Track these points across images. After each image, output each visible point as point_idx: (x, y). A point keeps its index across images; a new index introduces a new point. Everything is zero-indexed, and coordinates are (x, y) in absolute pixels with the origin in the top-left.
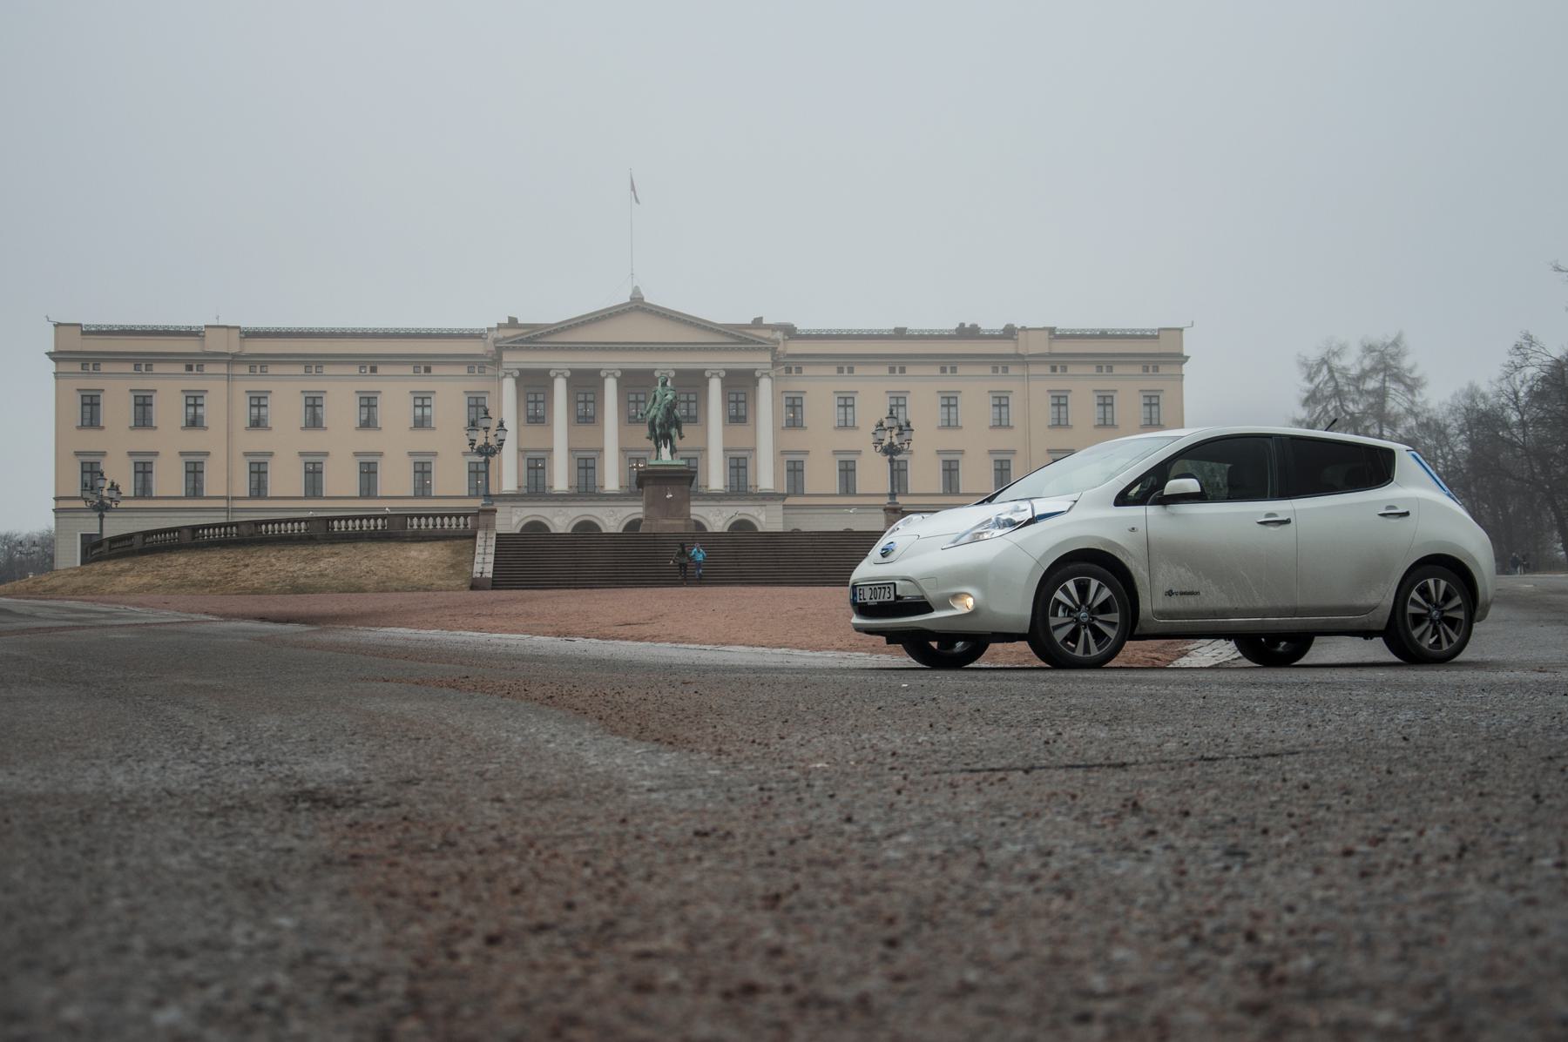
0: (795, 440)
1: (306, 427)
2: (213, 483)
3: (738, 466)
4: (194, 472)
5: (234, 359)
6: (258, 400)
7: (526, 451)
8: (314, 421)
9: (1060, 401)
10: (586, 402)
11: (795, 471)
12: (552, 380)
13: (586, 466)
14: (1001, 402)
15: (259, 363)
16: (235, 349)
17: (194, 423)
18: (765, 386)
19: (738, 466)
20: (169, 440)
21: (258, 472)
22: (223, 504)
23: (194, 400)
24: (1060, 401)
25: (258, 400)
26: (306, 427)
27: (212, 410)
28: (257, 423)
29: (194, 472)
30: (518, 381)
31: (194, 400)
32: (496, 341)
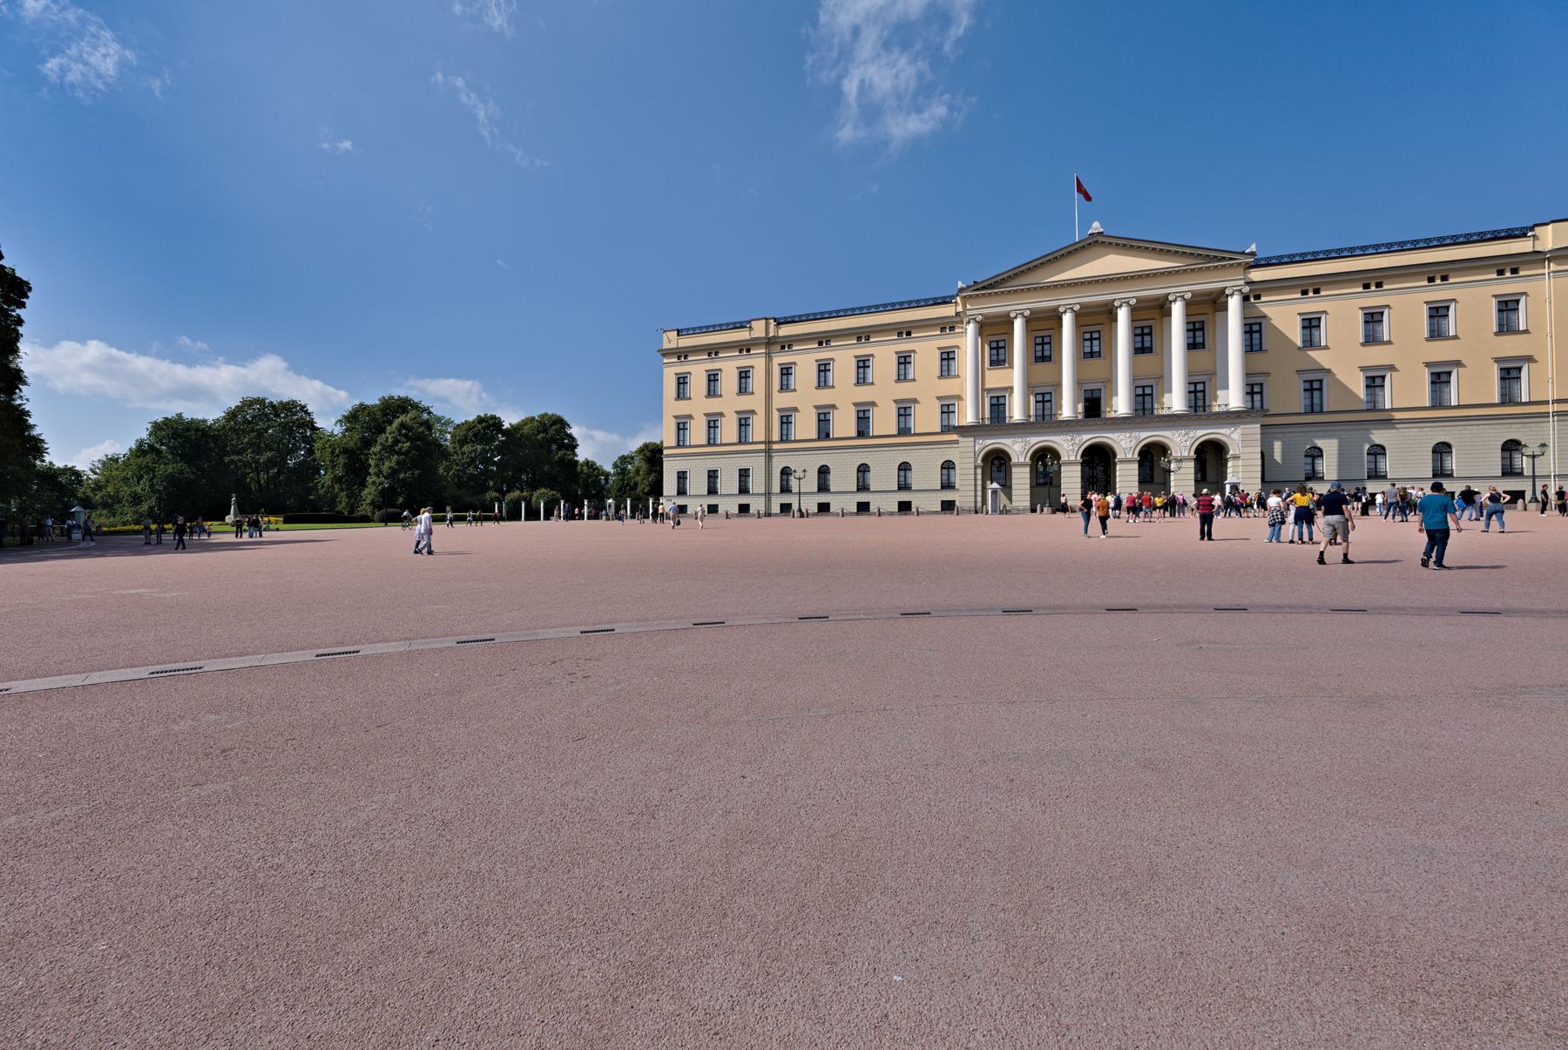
1: (819, 387)
2: (757, 431)
4: (743, 424)
5: (769, 342)
6: (786, 371)
7: (989, 390)
10: (1043, 344)
17: (743, 390)
20: (729, 402)
21: (786, 421)
22: (762, 447)
23: (744, 375)
26: (819, 387)
27: (757, 381)
28: (784, 387)
29: (743, 424)
31: (744, 375)
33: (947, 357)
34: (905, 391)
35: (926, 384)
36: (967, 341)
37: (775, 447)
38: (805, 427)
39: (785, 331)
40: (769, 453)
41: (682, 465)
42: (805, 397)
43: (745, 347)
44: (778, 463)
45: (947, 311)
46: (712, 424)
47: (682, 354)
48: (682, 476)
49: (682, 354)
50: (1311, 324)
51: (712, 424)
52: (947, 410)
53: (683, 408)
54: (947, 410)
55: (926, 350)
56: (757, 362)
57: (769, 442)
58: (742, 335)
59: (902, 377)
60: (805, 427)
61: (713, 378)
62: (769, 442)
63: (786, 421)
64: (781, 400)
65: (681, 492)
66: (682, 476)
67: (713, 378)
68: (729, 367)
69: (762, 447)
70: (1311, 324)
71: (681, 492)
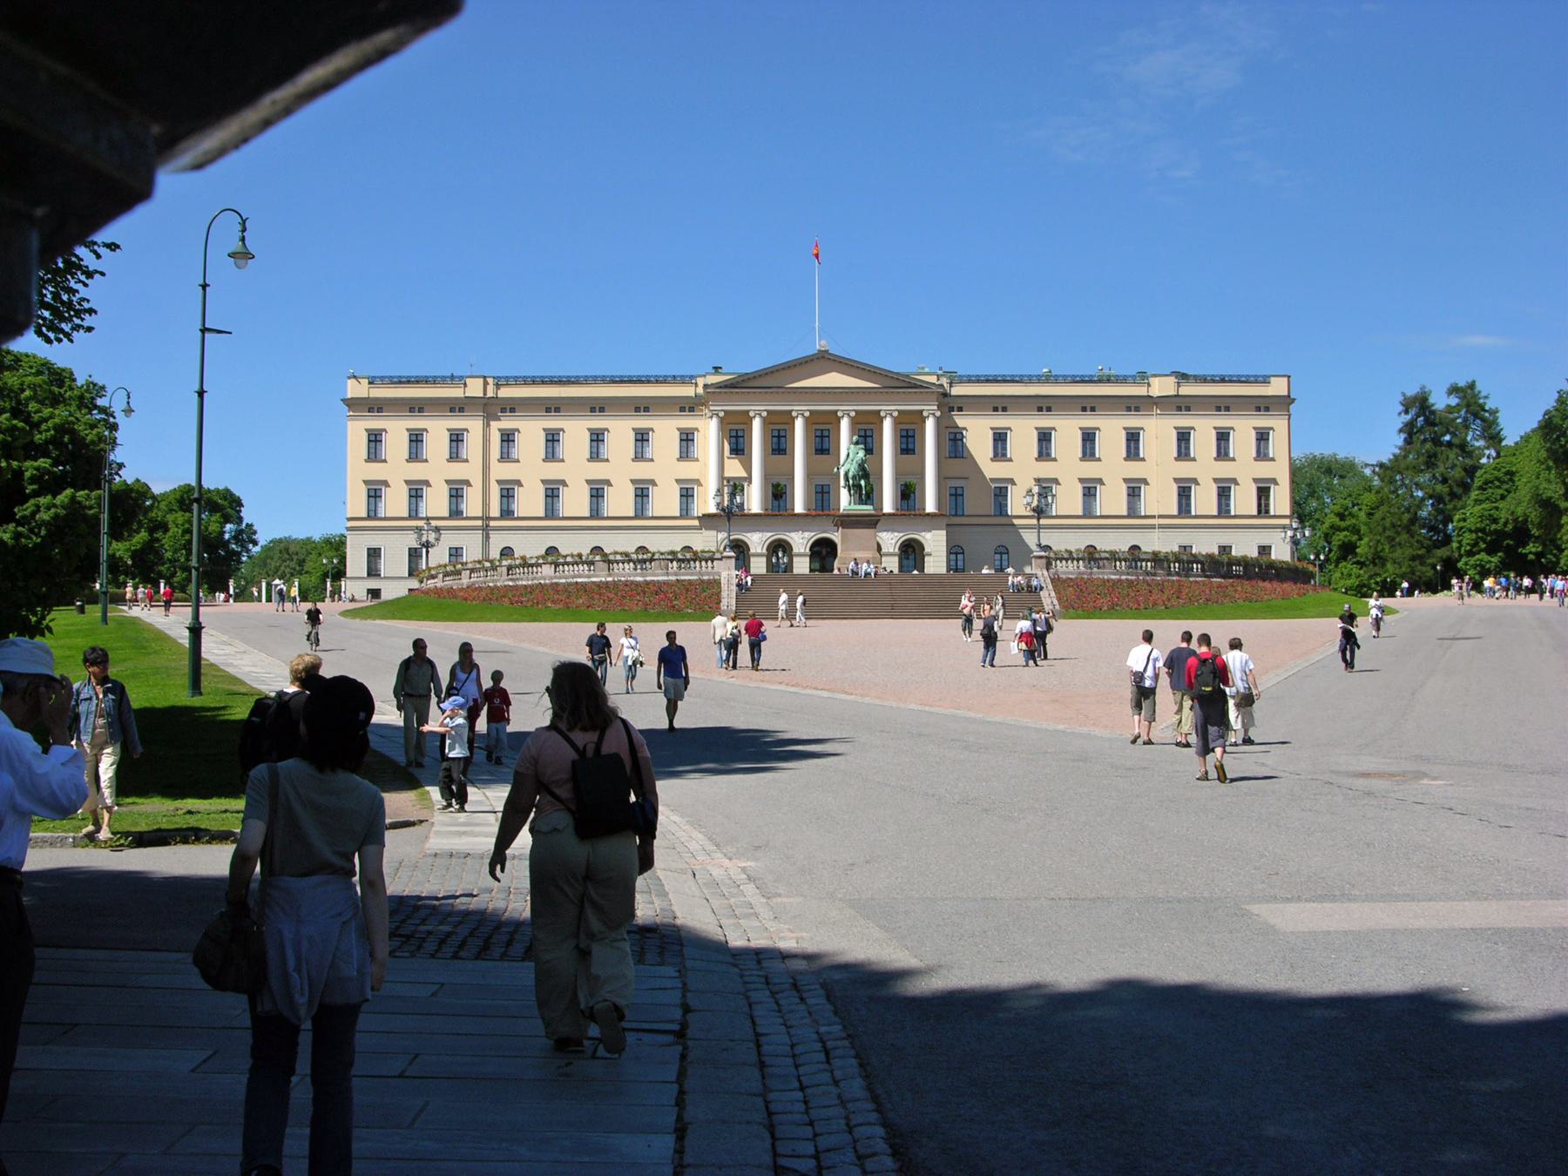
0: (956, 466)
2: (472, 504)
3: (908, 493)
6: (508, 438)
7: (729, 480)
8: (551, 455)
9: (1183, 437)
11: (957, 495)
12: (751, 419)
13: (778, 493)
14: (1133, 437)
15: (511, 407)
16: (490, 394)
17: (455, 456)
18: (930, 425)
19: (908, 493)
20: (437, 469)
21: (507, 494)
22: (479, 523)
23: (456, 438)
24: (1183, 437)
25: (508, 438)
28: (505, 457)
29: (456, 492)
30: (722, 421)
31: (456, 438)
32: (706, 386)
33: (687, 438)
34: (642, 471)
35: (665, 466)
36: (709, 431)
37: (492, 523)
38: (530, 502)
39: (505, 393)
40: (486, 530)
41: (374, 540)
42: (530, 467)
43: (457, 407)
44: (498, 542)
45: (687, 391)
46: (416, 492)
47: (374, 407)
48: (374, 554)
49: (374, 407)
50: (1000, 438)
51: (416, 492)
52: (687, 495)
53: (376, 471)
54: (687, 495)
55: (665, 430)
56: (473, 426)
57: (486, 518)
58: (455, 392)
59: (639, 456)
60: (530, 502)
61: (416, 439)
62: (486, 518)
63: (507, 494)
64: (501, 471)
65: (373, 572)
66: (374, 554)
67: (416, 439)
68: (437, 430)
69: (479, 523)
70: (1000, 438)
71: (373, 572)
